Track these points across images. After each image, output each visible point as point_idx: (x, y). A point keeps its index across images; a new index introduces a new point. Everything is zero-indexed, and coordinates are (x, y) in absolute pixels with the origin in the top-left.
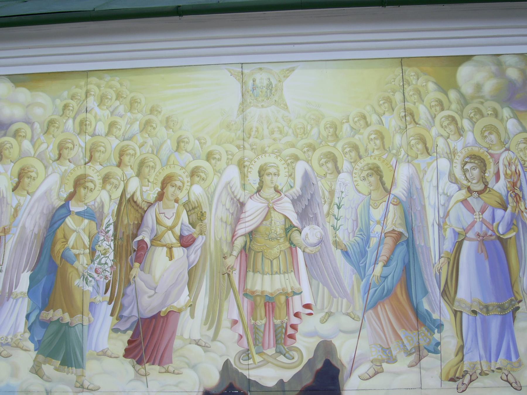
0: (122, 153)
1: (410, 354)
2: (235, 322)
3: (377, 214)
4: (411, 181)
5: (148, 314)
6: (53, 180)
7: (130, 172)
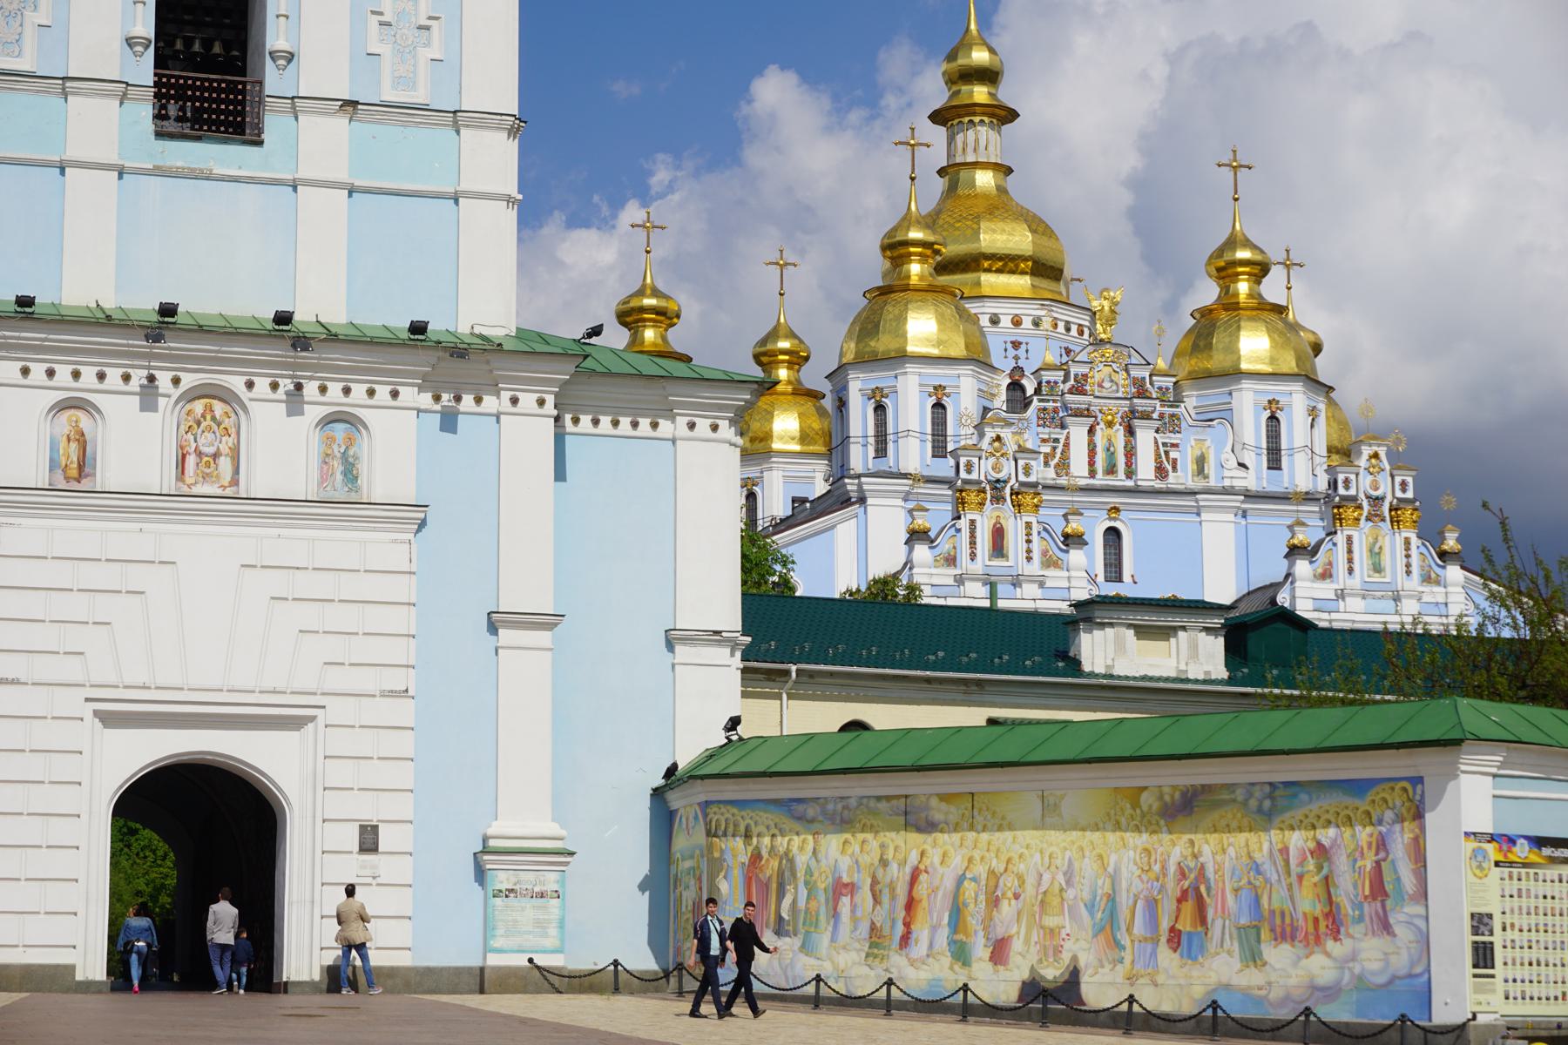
0: (989, 844)
1: (1110, 963)
2: (1036, 943)
3: (1100, 882)
4: (1116, 863)
5: (1000, 937)
6: (959, 858)
7: (993, 855)
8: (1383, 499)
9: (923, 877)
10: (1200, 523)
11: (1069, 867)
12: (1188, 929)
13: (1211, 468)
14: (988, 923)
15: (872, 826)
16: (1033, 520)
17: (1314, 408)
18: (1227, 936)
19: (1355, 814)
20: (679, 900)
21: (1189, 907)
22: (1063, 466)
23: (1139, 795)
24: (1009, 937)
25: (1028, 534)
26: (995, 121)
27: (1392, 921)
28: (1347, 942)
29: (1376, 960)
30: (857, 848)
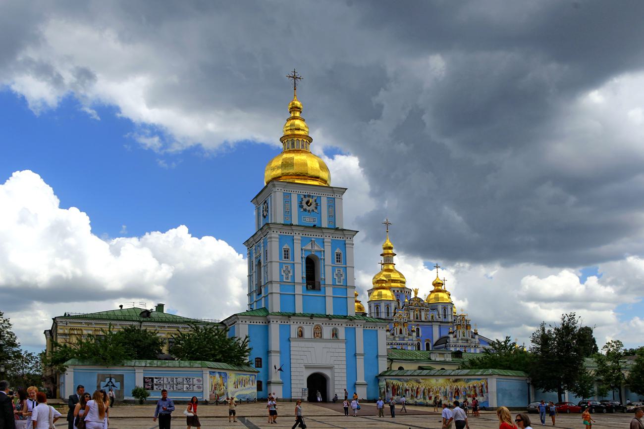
13: (434, 318)
14: (428, 395)
20: (380, 391)
22: (409, 318)
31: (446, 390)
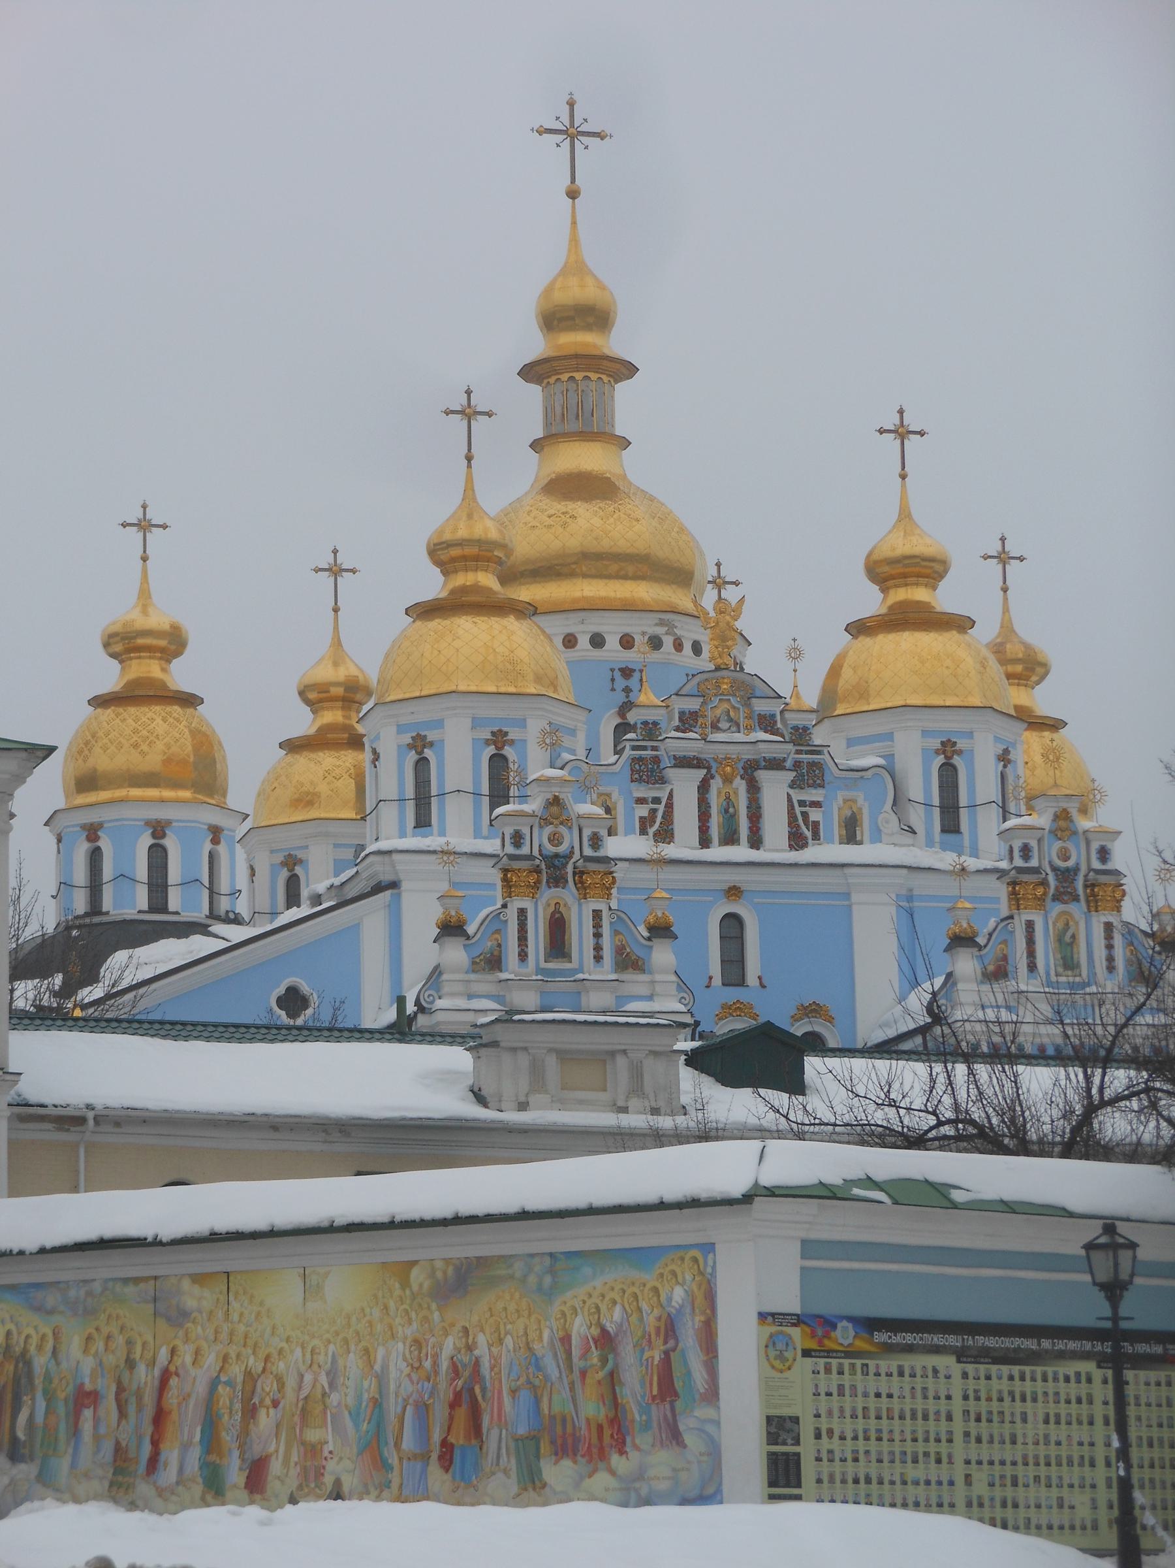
0: (246, 1337)
5: (256, 1457)
7: (250, 1351)
8: (1076, 870)
9: (173, 1382)
10: (850, 906)
11: (332, 1363)
12: (461, 1442)
15: (118, 1317)
16: (601, 905)
17: (1006, 751)
18: (504, 1451)
19: (642, 1291)
21: (462, 1413)
23: (411, 1269)
24: (266, 1457)
25: (597, 925)
26: (604, 377)
27: (682, 1427)
28: (633, 1455)
29: (664, 1478)
30: (101, 1345)
31: (381, 1380)
